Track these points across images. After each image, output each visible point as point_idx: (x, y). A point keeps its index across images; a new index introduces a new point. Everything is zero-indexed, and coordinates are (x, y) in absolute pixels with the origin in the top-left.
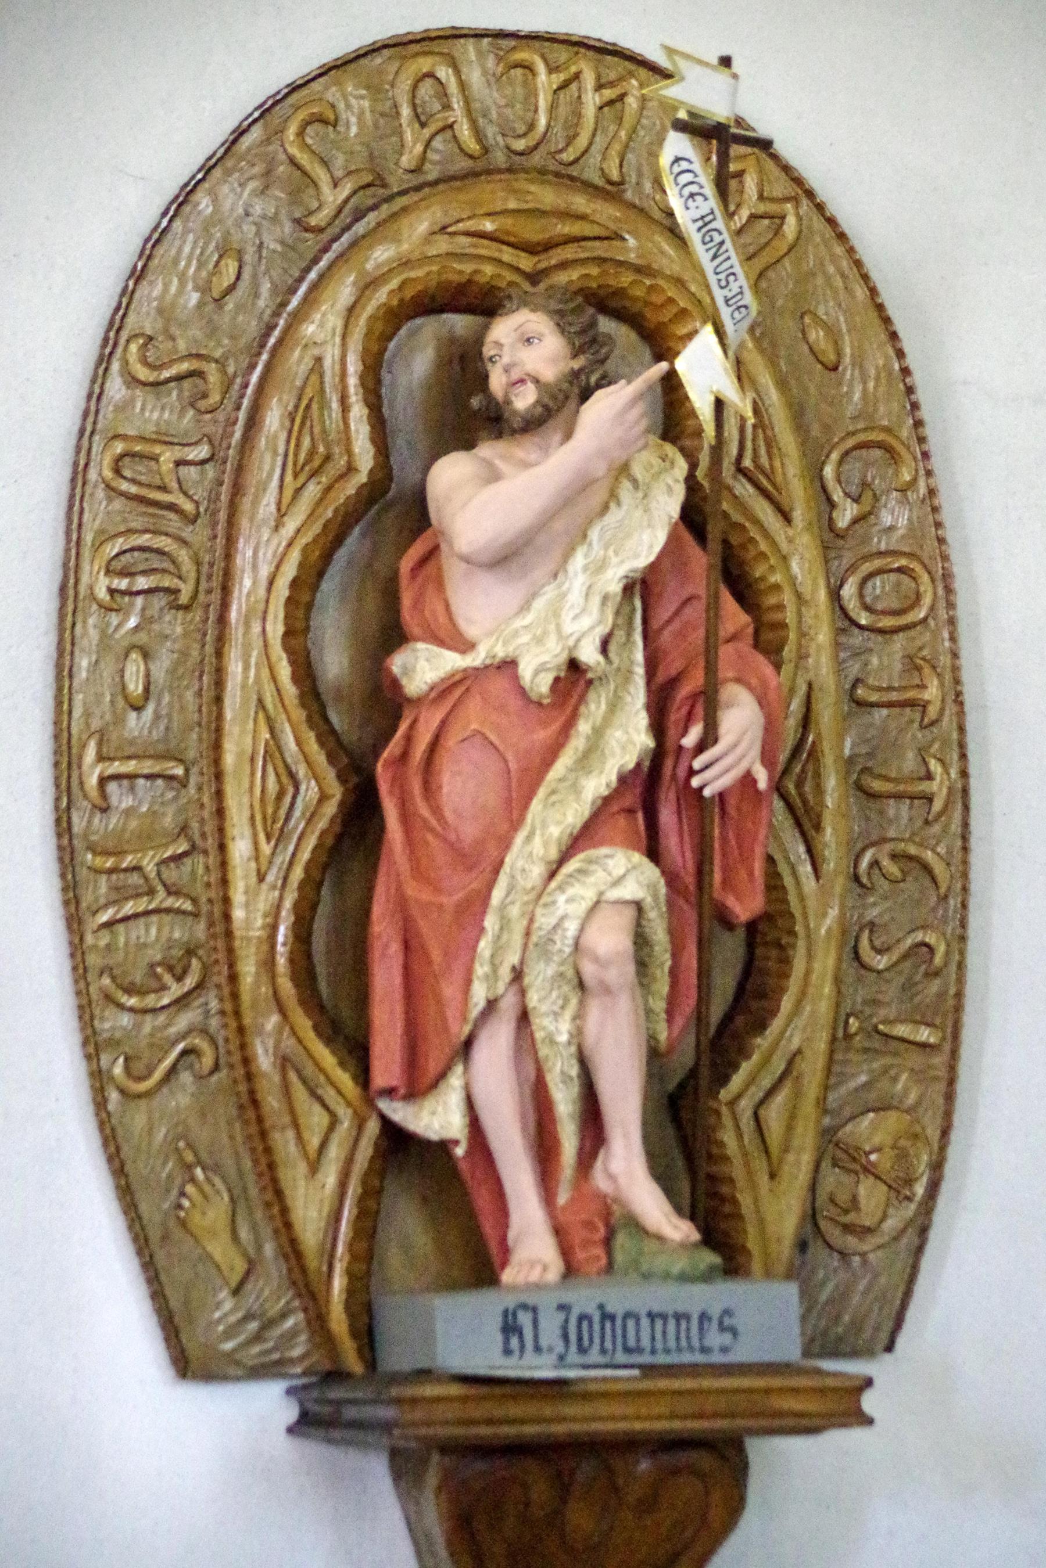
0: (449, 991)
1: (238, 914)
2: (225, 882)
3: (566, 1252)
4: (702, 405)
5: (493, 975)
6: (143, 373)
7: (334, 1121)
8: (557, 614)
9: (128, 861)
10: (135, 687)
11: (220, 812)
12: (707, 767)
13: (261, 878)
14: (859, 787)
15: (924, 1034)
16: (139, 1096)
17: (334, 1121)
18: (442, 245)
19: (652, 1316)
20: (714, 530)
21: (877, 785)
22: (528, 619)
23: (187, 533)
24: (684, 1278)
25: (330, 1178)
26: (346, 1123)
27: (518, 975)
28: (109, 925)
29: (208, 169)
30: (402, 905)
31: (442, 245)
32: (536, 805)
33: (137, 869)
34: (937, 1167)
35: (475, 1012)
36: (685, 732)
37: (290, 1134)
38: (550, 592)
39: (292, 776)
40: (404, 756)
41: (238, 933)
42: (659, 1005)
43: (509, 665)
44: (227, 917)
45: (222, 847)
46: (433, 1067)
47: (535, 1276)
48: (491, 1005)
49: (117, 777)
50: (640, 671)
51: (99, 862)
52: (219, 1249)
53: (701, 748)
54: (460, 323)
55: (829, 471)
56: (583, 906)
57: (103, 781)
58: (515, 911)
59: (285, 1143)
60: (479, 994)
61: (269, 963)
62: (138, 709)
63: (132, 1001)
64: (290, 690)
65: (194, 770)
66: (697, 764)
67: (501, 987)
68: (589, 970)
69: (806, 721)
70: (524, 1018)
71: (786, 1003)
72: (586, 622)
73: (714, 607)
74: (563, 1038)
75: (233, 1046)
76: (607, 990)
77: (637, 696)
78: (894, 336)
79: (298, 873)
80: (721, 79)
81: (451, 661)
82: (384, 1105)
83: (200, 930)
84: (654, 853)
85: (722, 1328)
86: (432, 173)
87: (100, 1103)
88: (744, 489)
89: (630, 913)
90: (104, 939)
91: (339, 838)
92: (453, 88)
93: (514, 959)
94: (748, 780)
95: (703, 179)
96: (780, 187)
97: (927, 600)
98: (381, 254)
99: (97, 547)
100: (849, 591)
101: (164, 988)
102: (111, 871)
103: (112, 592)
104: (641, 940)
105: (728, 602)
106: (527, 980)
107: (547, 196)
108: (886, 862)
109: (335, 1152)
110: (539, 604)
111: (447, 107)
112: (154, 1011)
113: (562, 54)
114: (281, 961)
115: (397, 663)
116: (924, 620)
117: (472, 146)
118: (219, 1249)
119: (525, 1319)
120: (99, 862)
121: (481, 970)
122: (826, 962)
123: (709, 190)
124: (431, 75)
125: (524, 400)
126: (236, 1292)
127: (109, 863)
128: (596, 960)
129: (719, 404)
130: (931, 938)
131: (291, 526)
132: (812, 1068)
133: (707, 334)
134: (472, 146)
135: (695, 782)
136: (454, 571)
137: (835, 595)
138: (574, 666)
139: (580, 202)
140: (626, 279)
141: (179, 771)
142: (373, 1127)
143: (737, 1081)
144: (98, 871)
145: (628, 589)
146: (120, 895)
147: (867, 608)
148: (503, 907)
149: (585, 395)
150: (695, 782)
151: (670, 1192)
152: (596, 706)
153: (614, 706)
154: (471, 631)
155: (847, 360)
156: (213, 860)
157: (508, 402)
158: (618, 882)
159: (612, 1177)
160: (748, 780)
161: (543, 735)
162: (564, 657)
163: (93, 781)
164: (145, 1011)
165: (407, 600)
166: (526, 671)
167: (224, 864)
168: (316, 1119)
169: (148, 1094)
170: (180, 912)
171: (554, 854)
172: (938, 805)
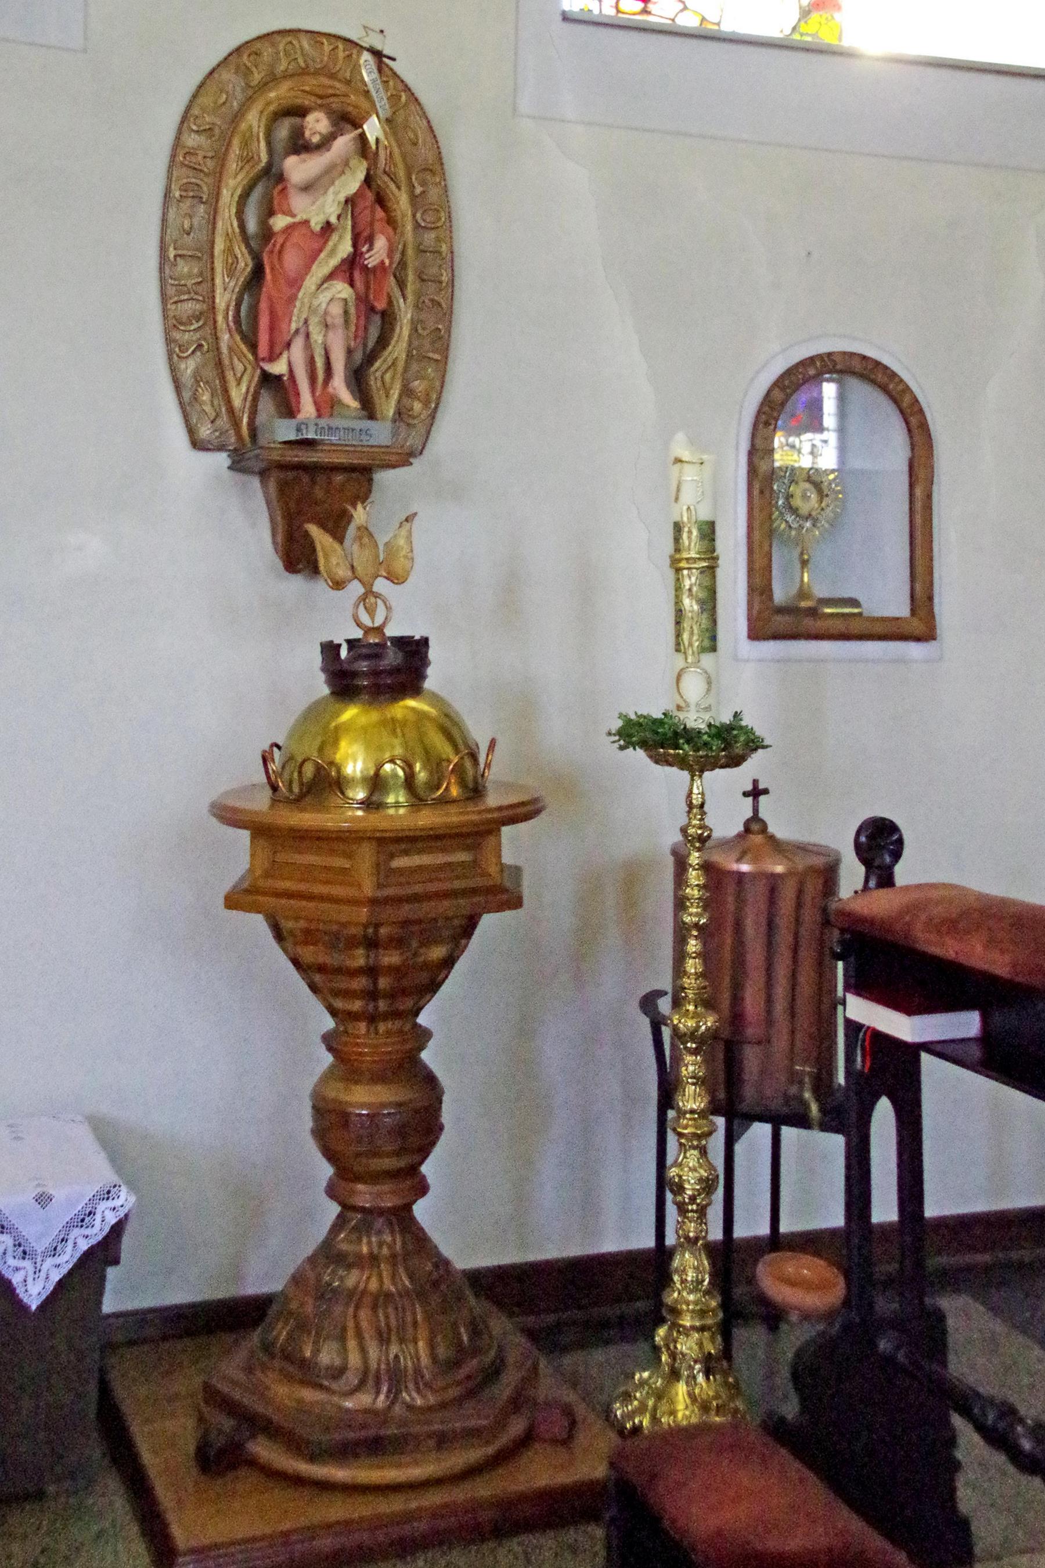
0: (284, 326)
1: (217, 301)
2: (213, 291)
3: (318, 410)
4: (371, 139)
5: (298, 321)
6: (195, 128)
7: (245, 369)
8: (324, 206)
9: (183, 282)
10: (186, 226)
11: (212, 269)
12: (370, 257)
13: (225, 290)
14: (420, 277)
15: (437, 357)
16: (184, 358)
17: (245, 369)
18: (292, 93)
19: (344, 429)
20: (374, 186)
21: (425, 277)
22: (314, 208)
23: (206, 180)
24: (355, 418)
25: (244, 389)
26: (249, 371)
27: (306, 322)
28: (176, 302)
29: (218, 65)
30: (270, 298)
31: (292, 93)
32: (314, 267)
33: (185, 285)
34: (439, 398)
35: (292, 332)
36: (363, 246)
37: (232, 373)
38: (321, 200)
39: (237, 258)
40: (272, 252)
41: (218, 328)
42: (352, 335)
43: (306, 222)
44: (214, 302)
45: (213, 279)
46: (277, 350)
47: (308, 415)
48: (297, 331)
49: (180, 256)
50: (349, 227)
51: (173, 282)
52: (207, 408)
53: (368, 251)
54: (298, 120)
55: (414, 177)
56: (328, 299)
57: (175, 256)
58: (306, 300)
59: (230, 376)
60: (293, 326)
61: (226, 317)
62: (188, 234)
63: (182, 328)
64: (237, 230)
65: (205, 256)
66: (367, 256)
67: (301, 324)
68: (329, 320)
69: (403, 253)
70: (308, 336)
71: (393, 342)
72: (332, 209)
73: (373, 212)
74: (320, 342)
75: (214, 345)
76: (334, 326)
77: (348, 236)
78: (435, 136)
79: (237, 290)
80: (380, 36)
81: (289, 220)
82: (262, 364)
83: (205, 306)
84: (352, 284)
85: (367, 434)
86: (290, 72)
87: (170, 359)
88: (386, 178)
89: (342, 304)
90: (173, 307)
91: (251, 280)
92: (297, 46)
93: (304, 316)
94: (382, 262)
95: (373, 67)
96: (400, 86)
97: (443, 219)
98: (272, 95)
99: (178, 180)
100: (418, 215)
101: (192, 324)
102: (176, 285)
103: (181, 196)
104: (346, 312)
105: (378, 209)
106: (309, 322)
107: (326, 81)
108: (427, 301)
109: (246, 379)
110: (318, 203)
111: (296, 53)
112: (189, 331)
113: (333, 40)
114: (230, 318)
115: (271, 221)
116: (442, 226)
117: (302, 64)
118: (207, 408)
119: (303, 427)
120: (173, 282)
121: (294, 318)
122: (406, 332)
123: (376, 71)
124: (291, 43)
125: (316, 139)
126: (212, 422)
127: (176, 283)
128: (332, 317)
129: (377, 140)
130: (440, 327)
131: (240, 177)
132: (401, 364)
133: (374, 118)
134: (302, 64)
135: (366, 262)
136: (292, 192)
137: (414, 216)
138: (328, 223)
139: (338, 85)
140: (350, 109)
141: (200, 255)
142: (259, 371)
143: (377, 364)
144: (172, 285)
145: (346, 202)
146: (180, 293)
147: (424, 220)
148: (302, 298)
149: (335, 138)
150: (366, 262)
151: (352, 392)
152: (335, 237)
153: (341, 237)
154: (295, 212)
155: (420, 141)
156: (209, 285)
157: (310, 140)
158: (339, 292)
159: (334, 389)
160: (382, 262)
161: (316, 246)
162: (324, 221)
163: (172, 256)
164: (185, 331)
165: (276, 202)
166: (313, 224)
167: (213, 285)
168: (239, 367)
169: (186, 357)
170: (198, 300)
171: (319, 282)
172: (444, 284)
